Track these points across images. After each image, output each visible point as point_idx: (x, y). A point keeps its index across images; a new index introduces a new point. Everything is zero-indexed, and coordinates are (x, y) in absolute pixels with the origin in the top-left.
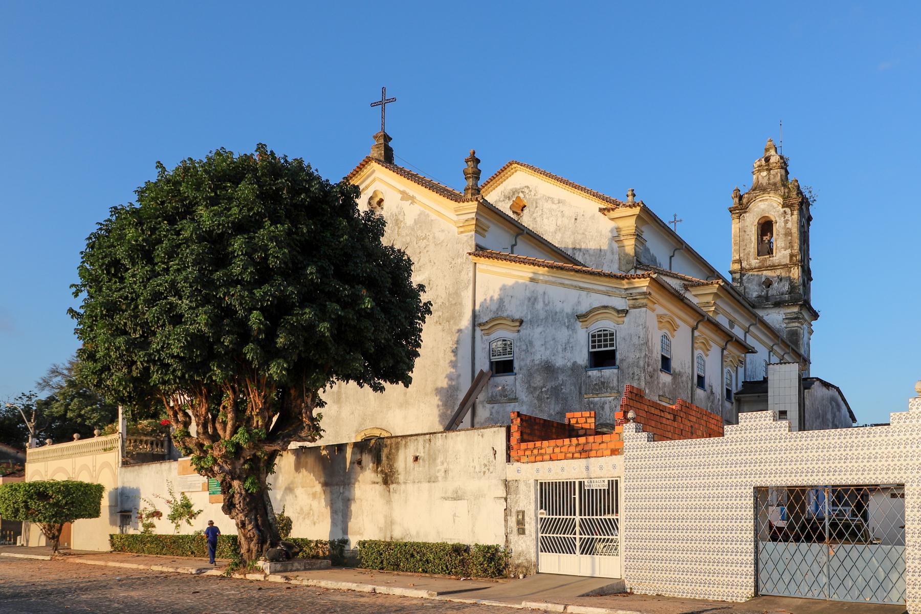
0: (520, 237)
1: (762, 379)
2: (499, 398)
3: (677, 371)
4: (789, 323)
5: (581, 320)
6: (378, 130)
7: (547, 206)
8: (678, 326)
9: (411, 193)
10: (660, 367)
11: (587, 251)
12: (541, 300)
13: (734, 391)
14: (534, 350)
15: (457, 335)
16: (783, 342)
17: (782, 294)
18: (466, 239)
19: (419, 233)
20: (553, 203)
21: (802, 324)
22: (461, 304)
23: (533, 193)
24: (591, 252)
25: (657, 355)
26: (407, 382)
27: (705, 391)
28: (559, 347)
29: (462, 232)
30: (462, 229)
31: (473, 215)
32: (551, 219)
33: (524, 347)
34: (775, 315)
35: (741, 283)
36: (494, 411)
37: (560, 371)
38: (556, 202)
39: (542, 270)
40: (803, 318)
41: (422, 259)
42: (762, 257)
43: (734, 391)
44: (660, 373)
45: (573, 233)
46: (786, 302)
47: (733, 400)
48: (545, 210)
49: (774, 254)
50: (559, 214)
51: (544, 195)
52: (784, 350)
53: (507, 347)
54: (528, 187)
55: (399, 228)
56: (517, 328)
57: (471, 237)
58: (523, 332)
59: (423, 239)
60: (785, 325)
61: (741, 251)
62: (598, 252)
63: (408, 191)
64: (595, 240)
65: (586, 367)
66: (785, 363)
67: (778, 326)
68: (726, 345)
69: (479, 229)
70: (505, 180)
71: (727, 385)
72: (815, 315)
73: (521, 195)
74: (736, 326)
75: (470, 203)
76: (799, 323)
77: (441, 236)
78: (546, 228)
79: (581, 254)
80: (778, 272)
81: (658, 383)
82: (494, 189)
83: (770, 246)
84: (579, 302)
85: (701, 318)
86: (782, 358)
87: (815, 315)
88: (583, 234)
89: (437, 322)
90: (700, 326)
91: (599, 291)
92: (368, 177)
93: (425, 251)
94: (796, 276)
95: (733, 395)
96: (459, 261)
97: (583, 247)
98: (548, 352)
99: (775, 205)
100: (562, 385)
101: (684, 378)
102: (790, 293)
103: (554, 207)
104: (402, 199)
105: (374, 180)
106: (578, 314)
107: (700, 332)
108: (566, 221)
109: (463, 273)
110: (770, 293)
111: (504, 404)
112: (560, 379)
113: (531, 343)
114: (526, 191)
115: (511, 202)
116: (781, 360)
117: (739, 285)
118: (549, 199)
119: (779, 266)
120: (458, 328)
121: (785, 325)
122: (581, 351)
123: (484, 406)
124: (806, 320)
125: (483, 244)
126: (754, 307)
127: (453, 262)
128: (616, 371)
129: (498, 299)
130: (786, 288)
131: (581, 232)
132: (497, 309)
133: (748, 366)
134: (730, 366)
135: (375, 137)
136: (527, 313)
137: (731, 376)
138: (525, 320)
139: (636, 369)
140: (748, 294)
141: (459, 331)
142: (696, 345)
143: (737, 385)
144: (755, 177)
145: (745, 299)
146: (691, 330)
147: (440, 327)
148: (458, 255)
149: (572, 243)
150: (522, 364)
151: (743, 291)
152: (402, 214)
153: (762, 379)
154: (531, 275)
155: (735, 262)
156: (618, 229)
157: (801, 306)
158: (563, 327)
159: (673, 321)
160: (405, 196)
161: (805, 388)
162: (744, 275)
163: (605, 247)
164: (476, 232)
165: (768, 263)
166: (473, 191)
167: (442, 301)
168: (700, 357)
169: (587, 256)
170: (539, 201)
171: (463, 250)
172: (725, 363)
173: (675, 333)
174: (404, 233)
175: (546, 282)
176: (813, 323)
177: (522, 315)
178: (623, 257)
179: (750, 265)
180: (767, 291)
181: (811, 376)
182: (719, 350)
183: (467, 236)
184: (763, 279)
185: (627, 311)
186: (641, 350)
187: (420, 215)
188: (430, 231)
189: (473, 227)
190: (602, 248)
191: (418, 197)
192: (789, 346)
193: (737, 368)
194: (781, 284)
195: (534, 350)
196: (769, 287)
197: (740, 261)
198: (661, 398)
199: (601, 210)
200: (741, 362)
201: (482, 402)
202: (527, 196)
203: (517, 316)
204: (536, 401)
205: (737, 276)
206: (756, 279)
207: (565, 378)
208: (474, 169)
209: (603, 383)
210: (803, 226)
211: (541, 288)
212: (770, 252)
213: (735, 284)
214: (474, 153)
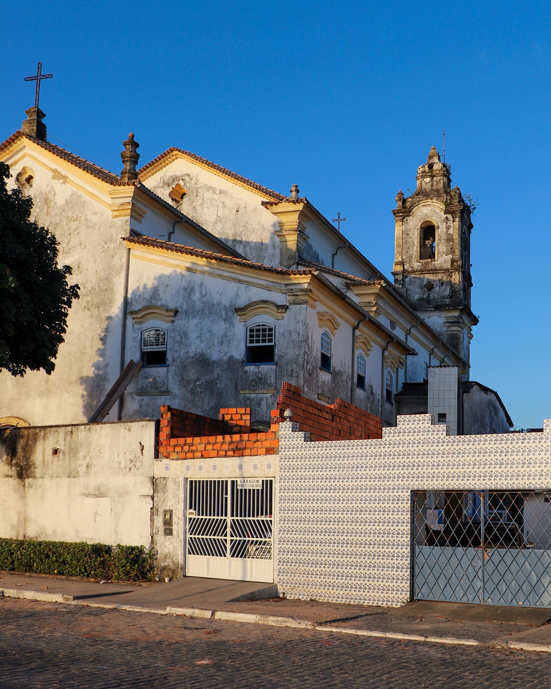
0: (178, 225)
1: (422, 381)
2: (149, 389)
3: (337, 369)
4: (449, 327)
5: (239, 313)
6: (32, 106)
7: (208, 195)
8: (339, 325)
9: (64, 173)
10: (319, 365)
11: (248, 243)
12: (197, 291)
13: (394, 392)
14: (188, 342)
15: (107, 322)
16: (443, 345)
17: (443, 298)
18: (120, 223)
19: (70, 214)
20: (214, 193)
21: (462, 329)
22: (112, 290)
23: (193, 182)
24: (252, 245)
25: (317, 352)
26: (50, 368)
27: (365, 391)
28: (216, 340)
29: (116, 216)
30: (116, 213)
31: (129, 200)
32: (212, 209)
33: (178, 338)
34: (436, 318)
35: (403, 284)
36: (143, 403)
37: (215, 365)
38: (217, 192)
39: (202, 261)
40: (463, 323)
41: (72, 241)
42: (424, 261)
43: (394, 392)
44: (320, 371)
45: (234, 225)
46: (447, 305)
47: (393, 401)
48: (205, 199)
49: (436, 259)
50: (221, 205)
51: (205, 185)
52: (443, 353)
53: (160, 337)
54: (189, 175)
55: (49, 207)
56: (171, 319)
57: (126, 222)
58: (178, 323)
59: (74, 221)
60: (446, 329)
61: (404, 253)
62: (260, 245)
63: (60, 169)
64: (256, 233)
65: (243, 362)
66: (445, 367)
67: (438, 329)
68: (387, 346)
69: (134, 214)
70: (165, 166)
71: (387, 385)
72: (475, 321)
73: (181, 183)
74: (397, 328)
75: (127, 187)
76: (459, 327)
77: (94, 219)
78: (206, 217)
79: (242, 246)
80: (440, 276)
81: (317, 381)
82: (153, 174)
83: (432, 250)
84: (237, 295)
85: (362, 318)
86: (442, 361)
87: (475, 321)
88: (245, 226)
89: (85, 308)
90: (361, 326)
91: (258, 284)
92: (17, 152)
93: (76, 232)
94: (457, 281)
95: (393, 396)
96: (112, 245)
97: (244, 239)
98: (203, 345)
99: (438, 210)
100: (217, 379)
101: (344, 378)
102: (451, 298)
103: (215, 197)
104: (54, 178)
105: (24, 156)
106: (237, 307)
107: (361, 331)
108: (227, 212)
109: (116, 258)
110: (431, 296)
111: (155, 397)
112: (215, 373)
113: (186, 334)
114: (187, 179)
115: (170, 189)
116: (441, 363)
117: (401, 286)
118: (209, 188)
119: (440, 270)
120: (107, 315)
121: (446, 329)
122: (238, 345)
123: (132, 398)
124: (466, 325)
125: (138, 230)
126: (415, 309)
127: (106, 246)
128: (274, 367)
129: (151, 288)
130: (448, 292)
131: (242, 224)
132: (151, 298)
133: (408, 367)
134: (391, 367)
135: (27, 112)
136: (182, 303)
137: (391, 377)
138: (180, 310)
139: (294, 366)
140: (410, 296)
141: (109, 318)
142: (356, 345)
143: (397, 386)
144: (418, 182)
145: (407, 301)
146: (351, 329)
147: (88, 313)
148: (111, 240)
149: (233, 235)
150: (176, 355)
151: (405, 293)
152: (53, 193)
153: (422, 381)
154: (189, 265)
155: (397, 264)
156: (281, 224)
157: (461, 310)
158: (221, 320)
159: (334, 319)
160: (57, 175)
161: (464, 392)
162: (406, 277)
163: (266, 241)
164: (132, 217)
165: (430, 267)
166: (131, 175)
167: (92, 285)
168: (360, 357)
169: (247, 248)
170: (199, 190)
171: (117, 235)
172: (385, 364)
173: (336, 331)
174: (53, 213)
175: (203, 272)
176: (473, 327)
177: (177, 305)
178: (284, 251)
179: (412, 267)
180: (429, 294)
181: (470, 380)
182: (380, 350)
183: (122, 220)
184: (425, 282)
185: (287, 306)
186: (300, 347)
187: (72, 195)
188: (82, 213)
189: (129, 211)
190: (264, 242)
191: (71, 177)
192: (450, 350)
193: (397, 369)
194: (443, 288)
195: (188, 342)
196: (430, 290)
197: (402, 263)
198: (320, 397)
199: (263, 203)
200: (402, 364)
201: (131, 394)
202: (188, 184)
203: (172, 306)
204: (189, 395)
205: (400, 277)
206: (418, 281)
207: (220, 373)
208: (133, 153)
209: (260, 379)
210: (464, 233)
211: (198, 278)
212: (432, 256)
213: (397, 286)
214: (133, 136)
